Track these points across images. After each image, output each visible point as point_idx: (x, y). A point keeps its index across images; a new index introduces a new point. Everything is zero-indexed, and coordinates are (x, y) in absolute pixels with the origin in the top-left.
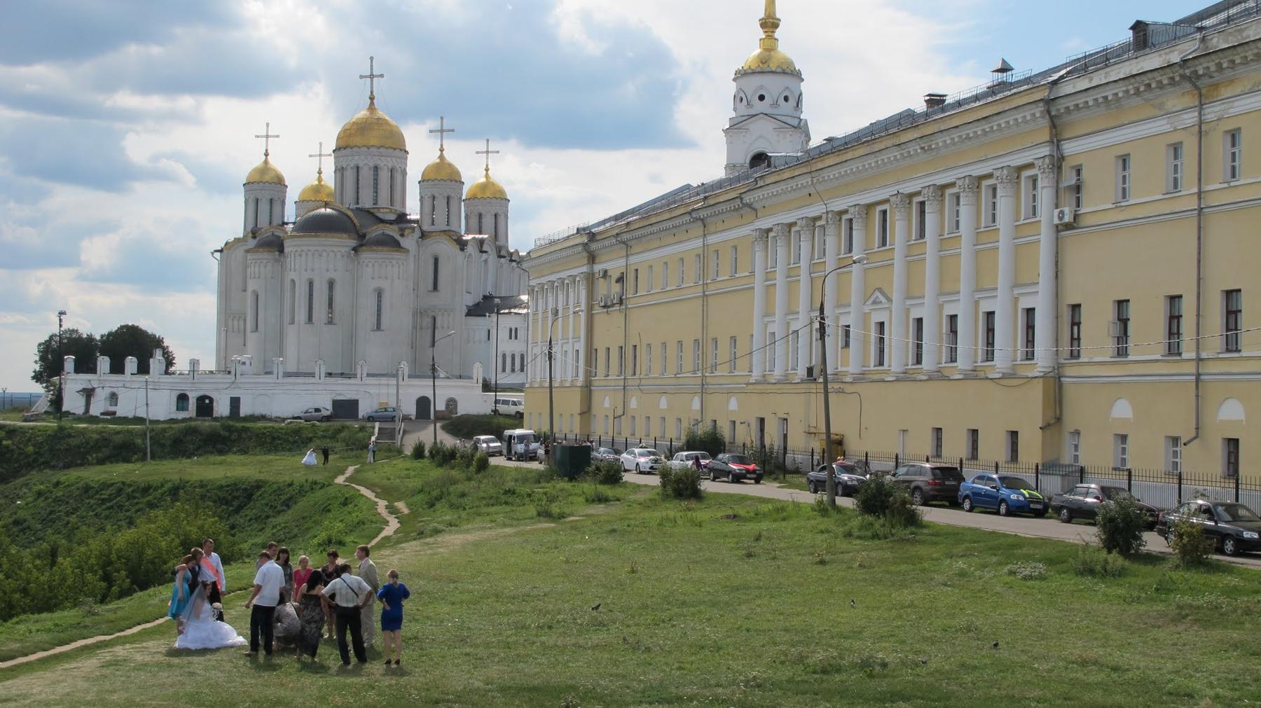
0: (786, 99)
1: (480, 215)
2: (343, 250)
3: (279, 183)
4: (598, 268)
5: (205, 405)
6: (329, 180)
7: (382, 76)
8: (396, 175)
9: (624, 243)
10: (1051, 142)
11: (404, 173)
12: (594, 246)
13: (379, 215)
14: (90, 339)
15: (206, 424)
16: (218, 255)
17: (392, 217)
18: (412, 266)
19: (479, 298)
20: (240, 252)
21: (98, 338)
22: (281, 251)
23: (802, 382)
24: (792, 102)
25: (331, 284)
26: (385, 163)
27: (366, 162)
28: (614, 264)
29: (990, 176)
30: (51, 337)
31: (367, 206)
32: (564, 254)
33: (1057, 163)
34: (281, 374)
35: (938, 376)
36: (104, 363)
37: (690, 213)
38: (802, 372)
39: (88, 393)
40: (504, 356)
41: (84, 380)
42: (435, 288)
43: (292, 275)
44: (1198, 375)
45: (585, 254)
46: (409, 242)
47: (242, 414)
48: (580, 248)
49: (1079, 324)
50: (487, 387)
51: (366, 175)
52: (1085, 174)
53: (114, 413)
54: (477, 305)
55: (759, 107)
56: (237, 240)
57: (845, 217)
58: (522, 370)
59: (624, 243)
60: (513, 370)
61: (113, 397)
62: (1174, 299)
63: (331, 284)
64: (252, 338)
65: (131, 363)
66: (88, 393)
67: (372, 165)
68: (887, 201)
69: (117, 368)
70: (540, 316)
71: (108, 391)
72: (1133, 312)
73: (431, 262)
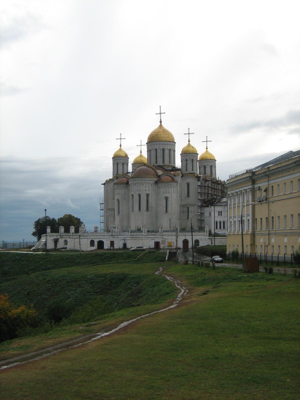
1: (205, 167)
2: (152, 182)
3: (126, 157)
4: (256, 186)
5: (101, 244)
6: (145, 154)
7: (164, 113)
8: (172, 151)
9: (267, 175)
11: (174, 151)
13: (166, 168)
14: (54, 220)
15: (100, 251)
17: (170, 168)
18: (179, 188)
20: (112, 184)
25: (148, 195)
27: (159, 147)
28: (263, 184)
30: (39, 219)
32: (243, 180)
36: (62, 229)
37: (295, 162)
39: (56, 241)
42: (188, 196)
45: (251, 180)
46: (179, 179)
48: (249, 178)
50: (210, 234)
51: (160, 153)
53: (66, 248)
56: (110, 180)
58: (224, 228)
59: (267, 175)
60: (220, 228)
61: (66, 242)
63: (148, 195)
64: (117, 218)
65: (72, 229)
66: (56, 241)
67: (161, 148)
69: (67, 230)
70: (232, 206)
71: (64, 239)
73: (186, 186)
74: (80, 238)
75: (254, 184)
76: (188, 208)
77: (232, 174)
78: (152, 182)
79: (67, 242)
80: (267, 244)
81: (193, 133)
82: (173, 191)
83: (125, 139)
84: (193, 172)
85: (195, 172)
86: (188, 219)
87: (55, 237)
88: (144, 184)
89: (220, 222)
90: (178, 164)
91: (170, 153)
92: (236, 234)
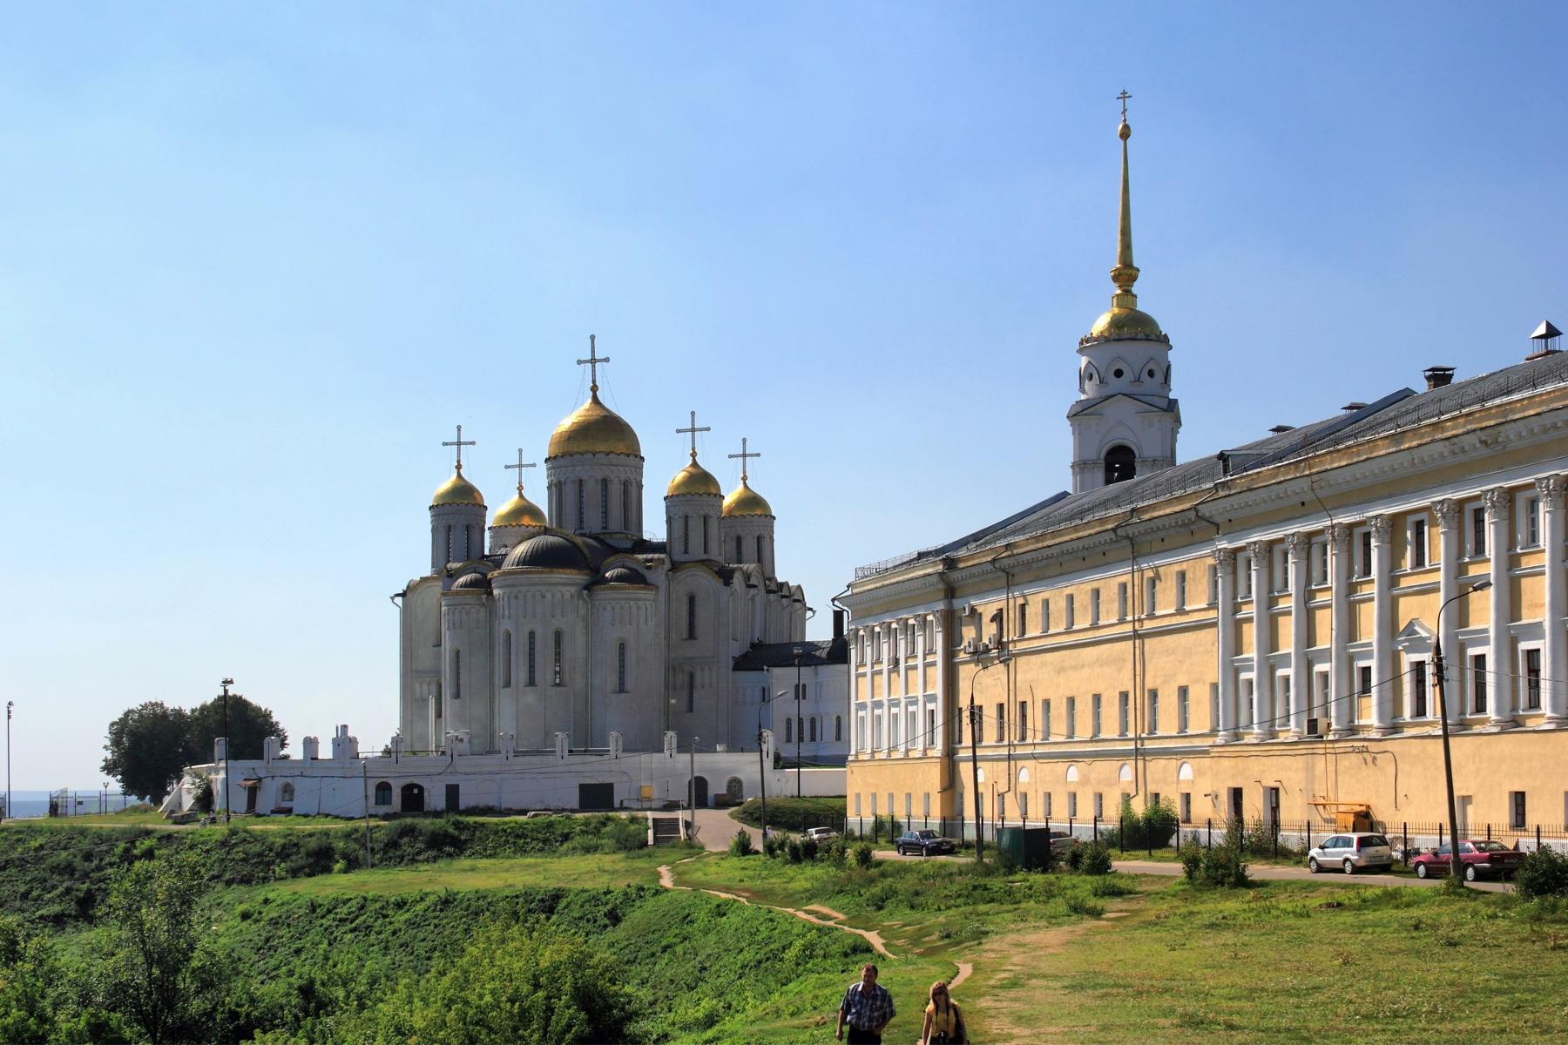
1: (739, 540)
2: (573, 589)
4: (957, 603)
5: (413, 798)
6: (540, 498)
7: (607, 360)
11: (640, 486)
12: (955, 575)
14: (179, 713)
16: (399, 600)
17: (628, 545)
19: (747, 648)
21: (188, 712)
22: (491, 593)
25: (558, 636)
26: (617, 475)
30: (127, 714)
31: (595, 531)
34: (511, 755)
40: (789, 721)
42: (692, 635)
43: (504, 625)
46: (658, 576)
47: (462, 807)
54: (745, 655)
56: (423, 580)
58: (813, 739)
61: (288, 790)
63: (558, 636)
67: (600, 477)
71: (280, 782)
73: (685, 600)
74: (366, 778)
75: (953, 597)
76: (692, 676)
77: (865, 564)
78: (573, 589)
79: (292, 792)
80: (1002, 787)
81: (708, 429)
82: (643, 619)
83: (473, 443)
84: (704, 557)
85: (717, 553)
86: (691, 709)
88: (549, 595)
89: (800, 721)
90: (655, 527)
91: (626, 492)
92: (867, 757)
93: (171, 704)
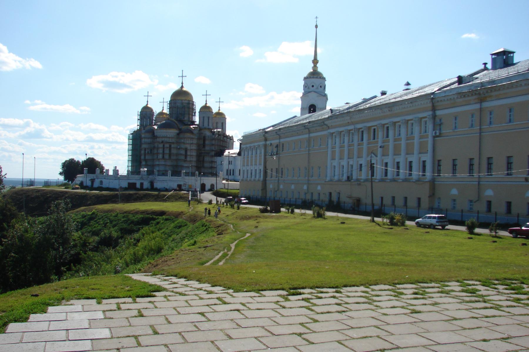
0: (321, 87)
1: (217, 123)
4: (268, 142)
10: (432, 110)
14: (78, 162)
23: (346, 181)
24: (323, 87)
29: (412, 120)
33: (434, 117)
35: (394, 180)
38: (345, 178)
39: (93, 181)
41: (92, 176)
44: (479, 182)
49: (440, 166)
52: (442, 121)
55: (312, 89)
57: (361, 130)
58: (233, 175)
60: (230, 175)
62: (471, 159)
66: (93, 181)
68: (376, 126)
71: (99, 180)
72: (457, 162)
80: (276, 189)
87: (92, 178)
90: (197, 119)
93: (76, 159)
